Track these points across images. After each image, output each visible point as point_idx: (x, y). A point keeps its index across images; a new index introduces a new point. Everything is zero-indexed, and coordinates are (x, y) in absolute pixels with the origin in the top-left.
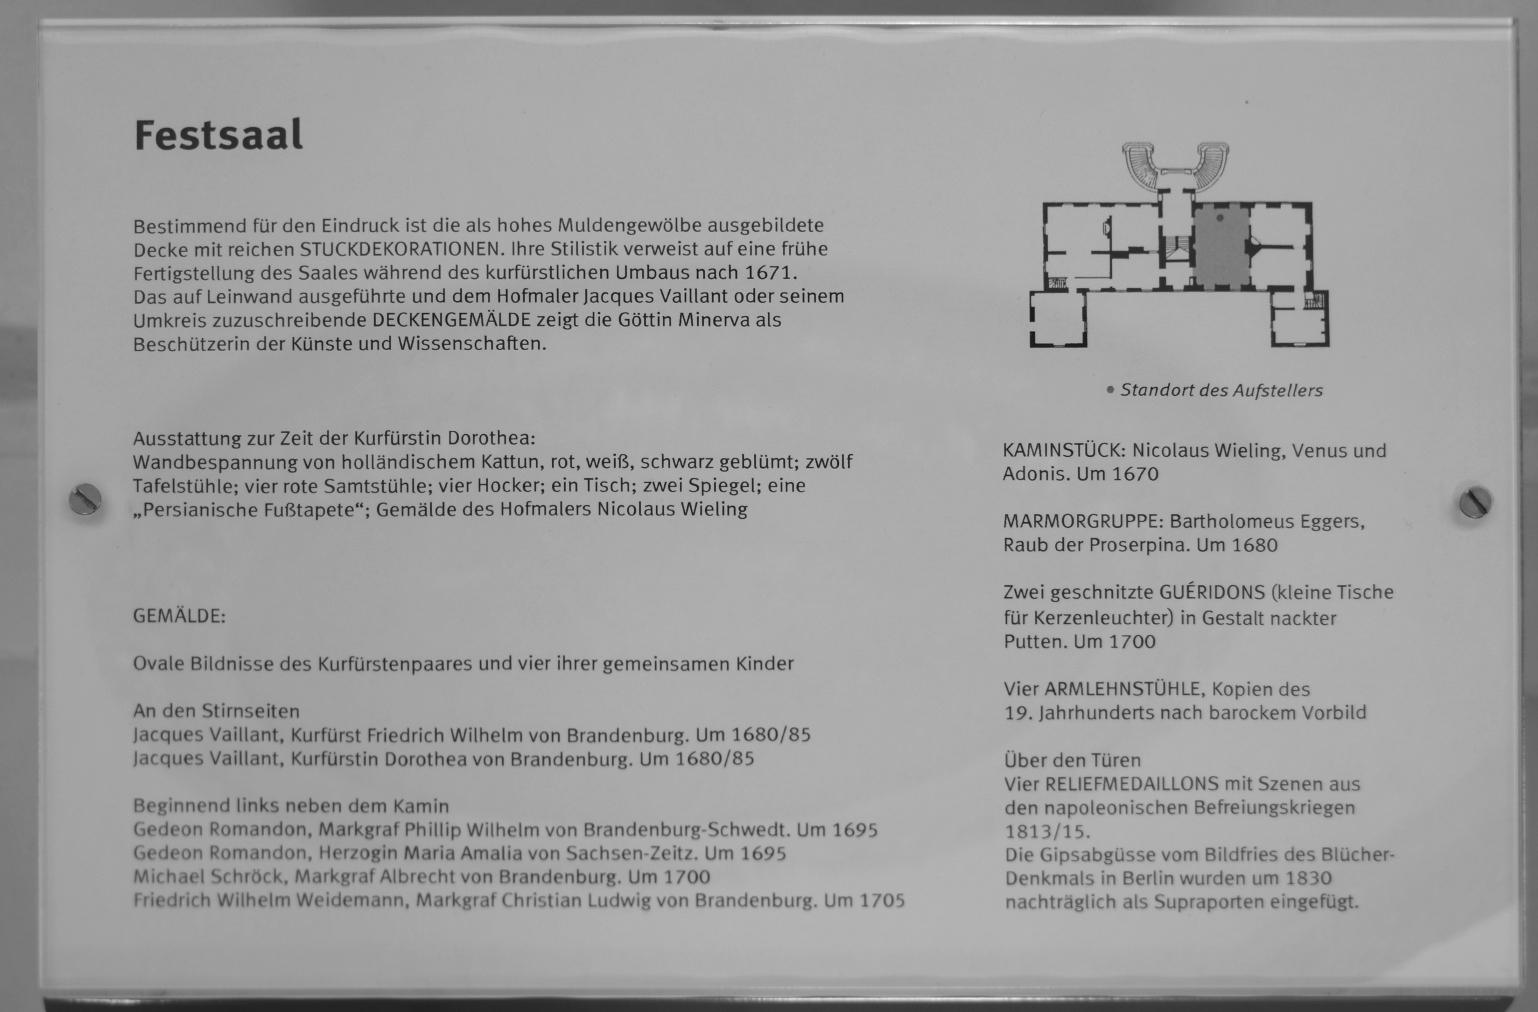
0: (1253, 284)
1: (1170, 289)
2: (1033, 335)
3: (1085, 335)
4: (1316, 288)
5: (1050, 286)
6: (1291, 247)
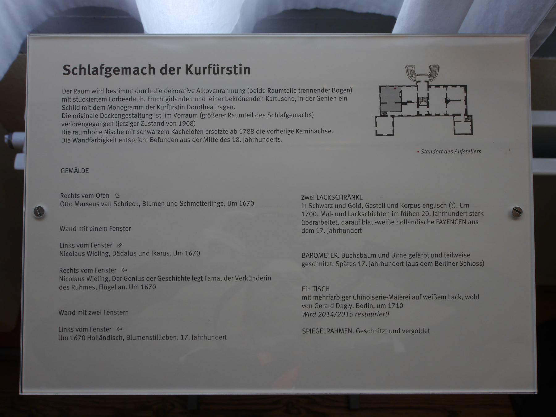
0: (448, 113)
1: (421, 115)
2: (376, 131)
3: (393, 131)
4: (468, 114)
5: (382, 115)
6: (460, 101)
